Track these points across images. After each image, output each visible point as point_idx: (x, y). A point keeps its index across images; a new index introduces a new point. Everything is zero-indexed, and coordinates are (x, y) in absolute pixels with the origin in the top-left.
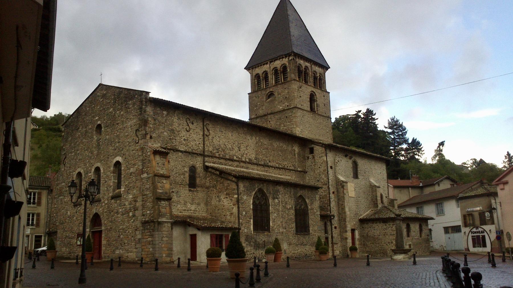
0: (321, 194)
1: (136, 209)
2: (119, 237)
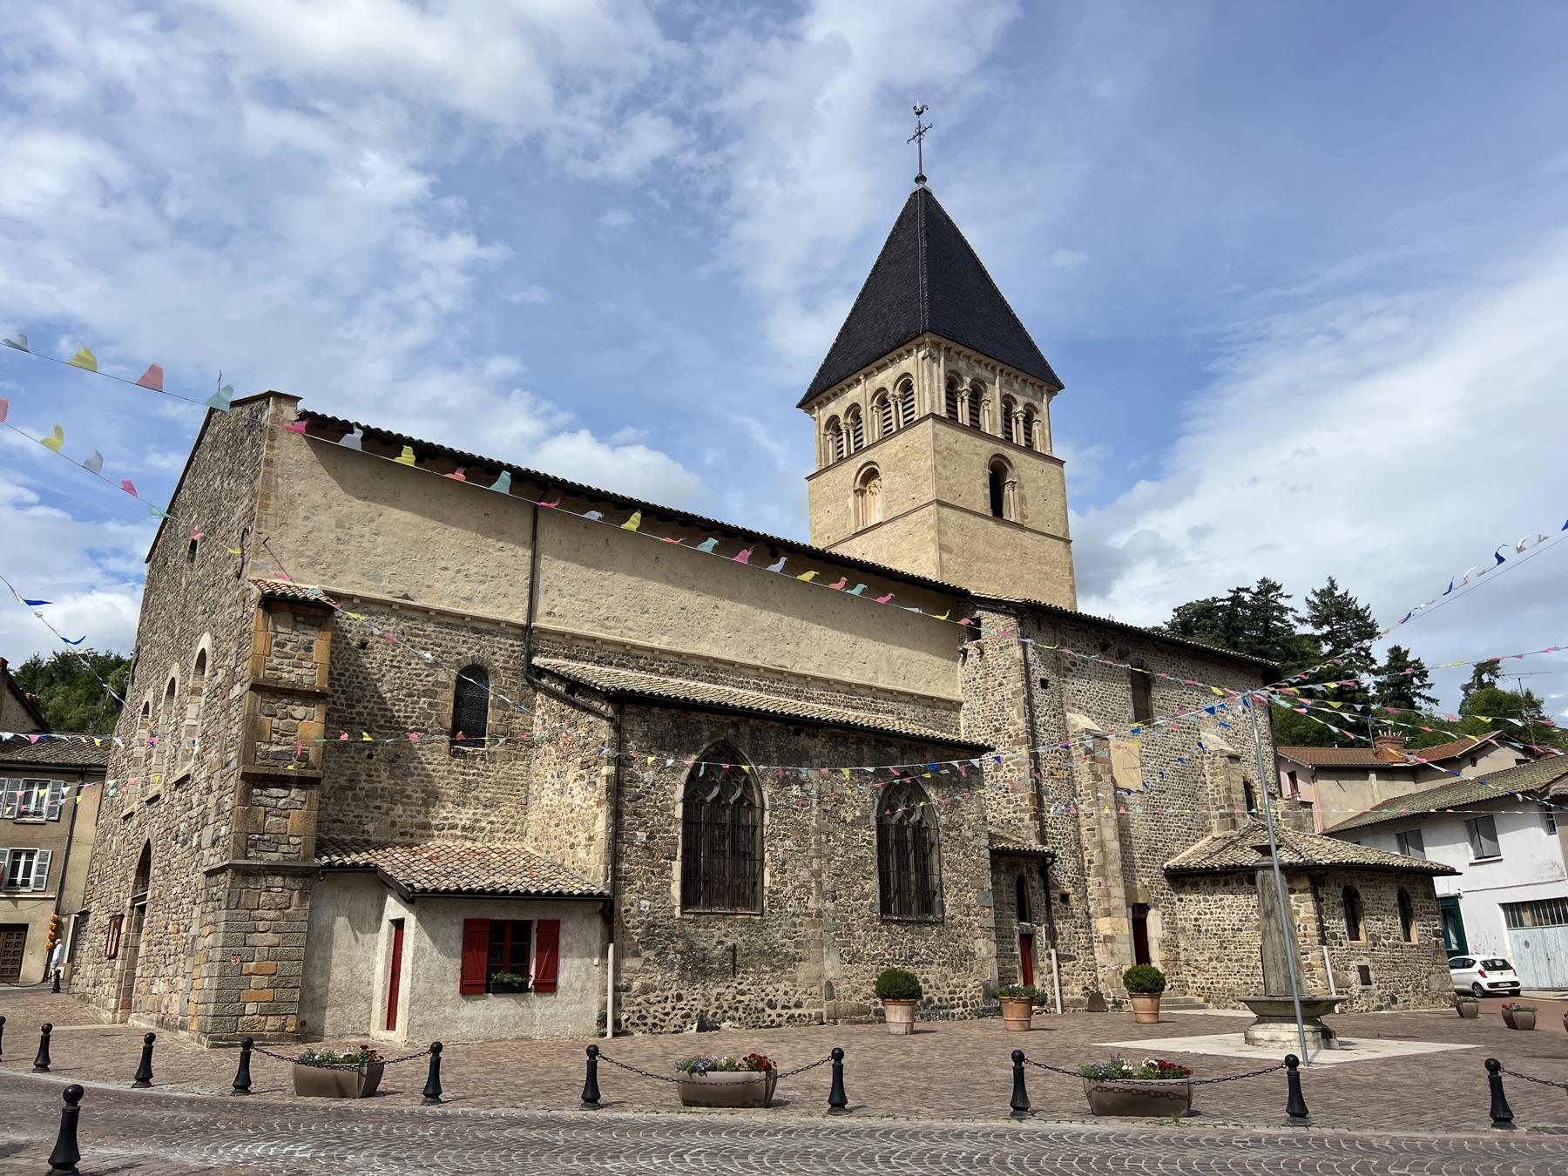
0: (1009, 775)
2: (166, 928)
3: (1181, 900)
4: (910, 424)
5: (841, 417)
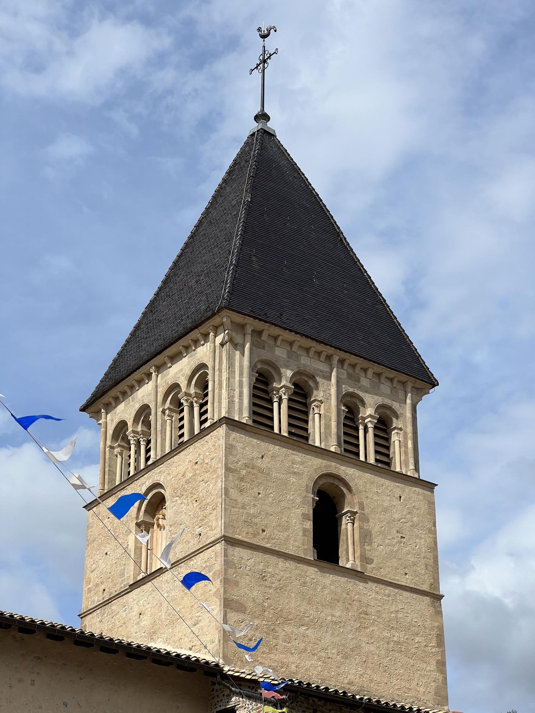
4: (204, 432)
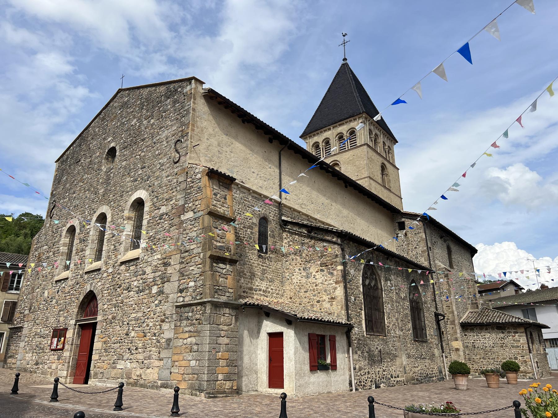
1: (165, 279)
2: (127, 334)
3: (466, 335)
5: (321, 143)
